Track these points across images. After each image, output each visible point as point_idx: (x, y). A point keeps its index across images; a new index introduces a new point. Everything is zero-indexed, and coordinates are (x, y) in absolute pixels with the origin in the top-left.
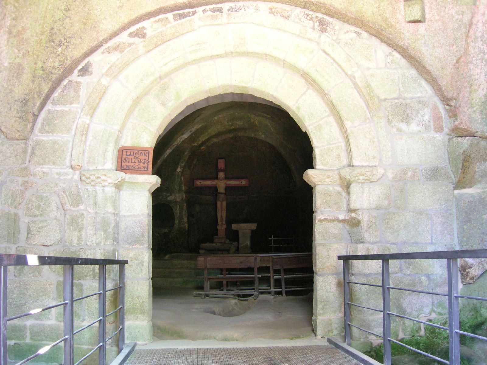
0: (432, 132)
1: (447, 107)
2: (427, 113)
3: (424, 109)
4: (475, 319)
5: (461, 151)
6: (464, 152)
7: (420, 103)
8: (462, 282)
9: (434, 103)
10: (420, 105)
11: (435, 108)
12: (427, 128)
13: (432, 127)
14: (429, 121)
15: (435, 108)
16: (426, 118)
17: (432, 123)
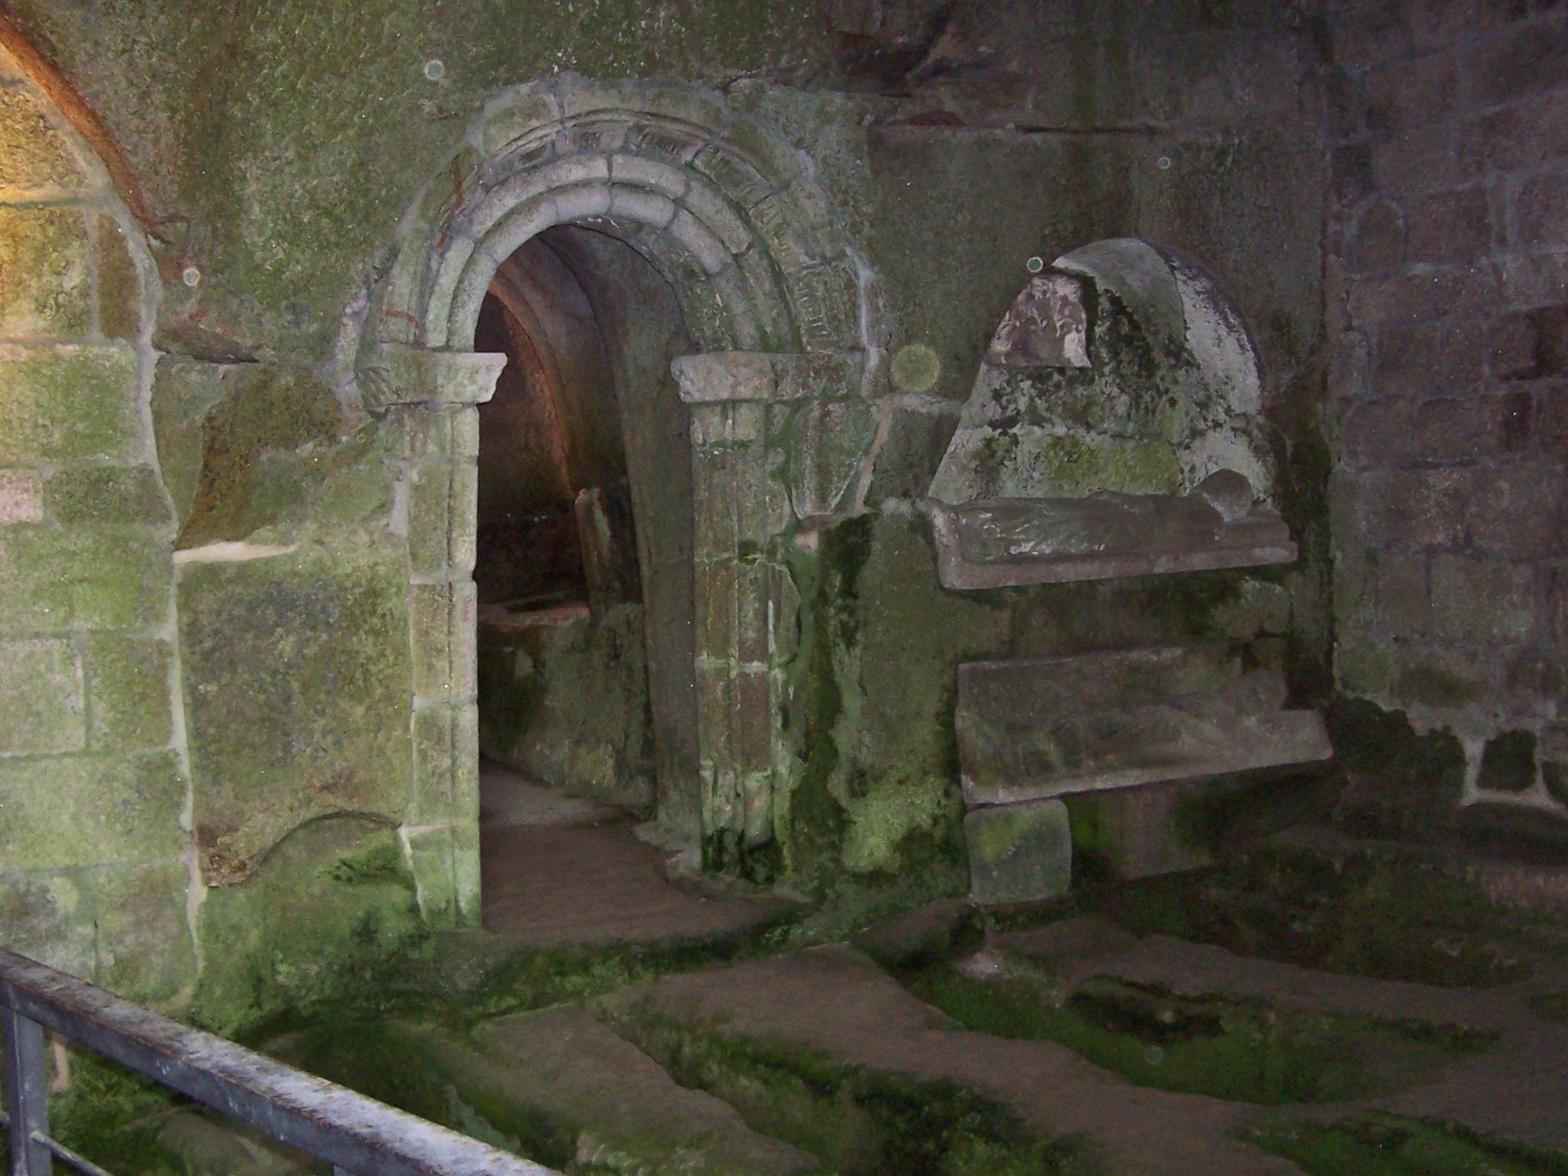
0: (96, 334)
1: (155, 243)
2: (78, 260)
3: (66, 247)
4: (251, 1007)
5: (199, 419)
6: (210, 419)
7: (52, 223)
8: (207, 881)
9: (107, 225)
10: (51, 231)
11: (112, 241)
12: (74, 324)
13: (96, 316)
14: (85, 295)
15: (112, 241)
16: (73, 279)
17: (95, 301)
